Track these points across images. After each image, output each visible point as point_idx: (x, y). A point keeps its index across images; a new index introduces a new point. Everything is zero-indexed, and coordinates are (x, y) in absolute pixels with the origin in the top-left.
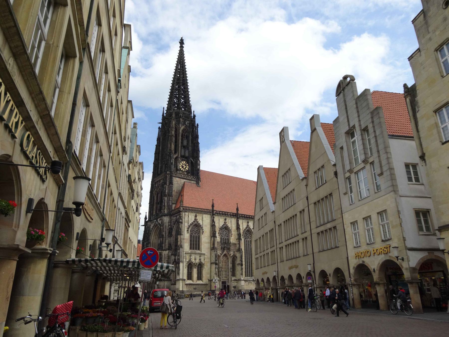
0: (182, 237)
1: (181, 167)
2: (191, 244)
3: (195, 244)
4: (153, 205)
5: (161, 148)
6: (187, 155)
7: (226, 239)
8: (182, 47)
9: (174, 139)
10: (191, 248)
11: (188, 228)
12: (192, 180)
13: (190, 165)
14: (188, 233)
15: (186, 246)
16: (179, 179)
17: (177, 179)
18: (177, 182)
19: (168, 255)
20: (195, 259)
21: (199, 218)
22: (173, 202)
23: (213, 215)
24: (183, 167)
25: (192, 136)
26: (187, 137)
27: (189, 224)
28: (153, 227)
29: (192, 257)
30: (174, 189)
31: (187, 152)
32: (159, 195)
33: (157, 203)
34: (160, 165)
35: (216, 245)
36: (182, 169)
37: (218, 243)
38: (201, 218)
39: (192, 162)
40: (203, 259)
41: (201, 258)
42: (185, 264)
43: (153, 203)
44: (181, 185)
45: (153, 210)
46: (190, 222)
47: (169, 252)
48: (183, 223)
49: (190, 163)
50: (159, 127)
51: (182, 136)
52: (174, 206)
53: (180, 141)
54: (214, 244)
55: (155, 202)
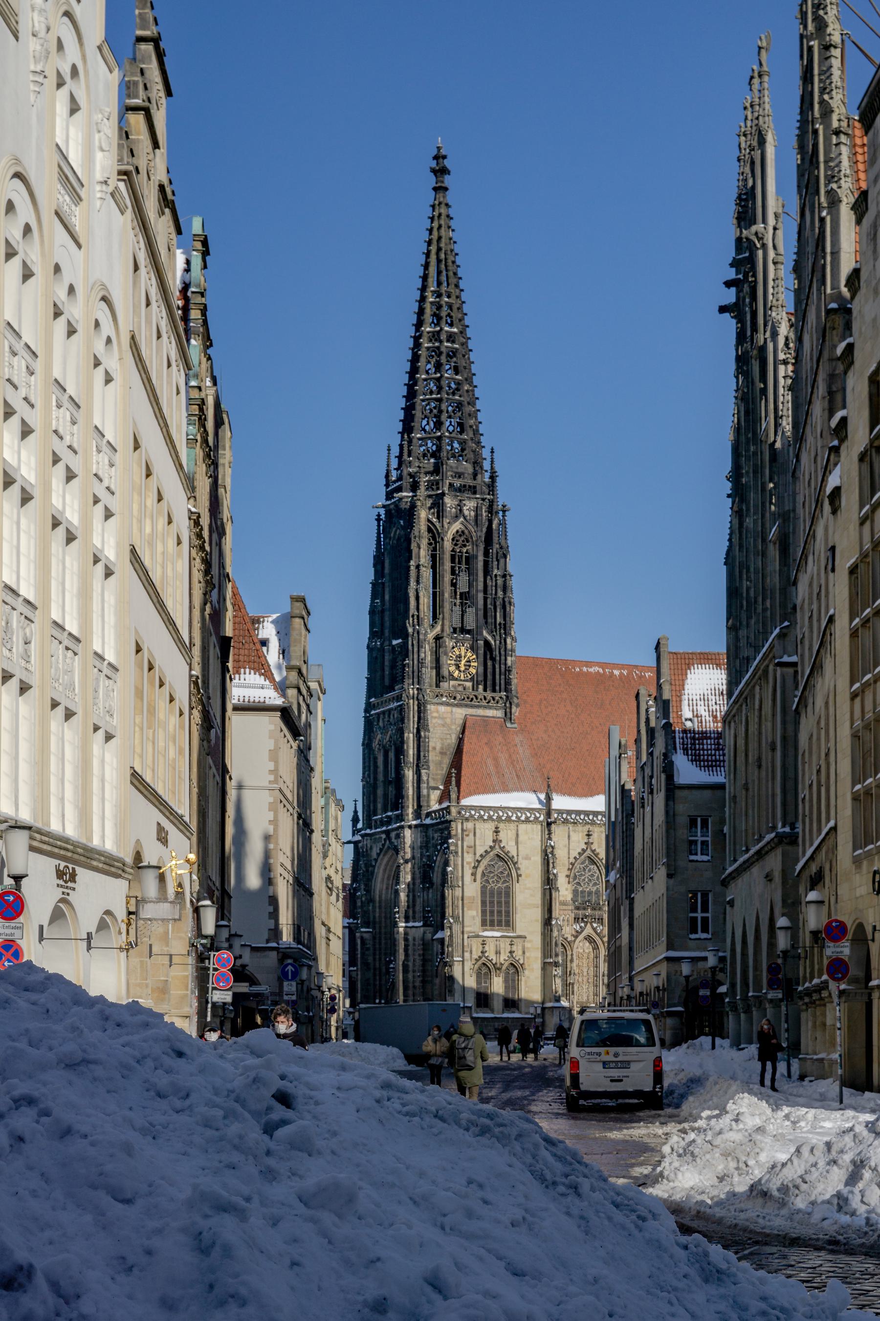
0: (458, 892)
1: (452, 668)
2: (484, 912)
3: (498, 910)
4: (375, 787)
5: (387, 597)
6: (470, 624)
7: (590, 893)
8: (439, 216)
9: (427, 574)
10: (484, 923)
11: (475, 868)
12: (490, 708)
13: (481, 659)
14: (475, 880)
15: (472, 917)
16: (449, 709)
17: (442, 709)
18: (443, 721)
19: (423, 939)
20: (498, 953)
21: (507, 836)
22: (432, 784)
23: (549, 824)
24: (458, 667)
25: (486, 554)
26: (469, 560)
27: (478, 855)
28: (378, 855)
29: (487, 948)
30: (431, 744)
31: (470, 612)
32: (392, 755)
33: (387, 783)
34: (387, 658)
35: (555, 914)
36: (456, 674)
37: (563, 903)
38: (511, 834)
39: (487, 643)
40: (520, 952)
41: (514, 948)
42: (468, 965)
43: (375, 779)
44: (456, 729)
45: (375, 801)
46: (480, 851)
47: (424, 933)
48: (460, 854)
49: (481, 652)
50: (379, 515)
51: (453, 561)
52: (435, 795)
53: (448, 577)
54: (550, 911)
55: (381, 777)
